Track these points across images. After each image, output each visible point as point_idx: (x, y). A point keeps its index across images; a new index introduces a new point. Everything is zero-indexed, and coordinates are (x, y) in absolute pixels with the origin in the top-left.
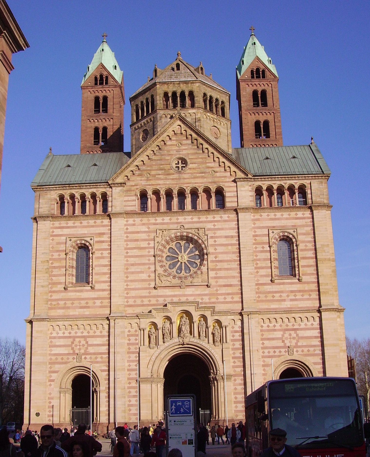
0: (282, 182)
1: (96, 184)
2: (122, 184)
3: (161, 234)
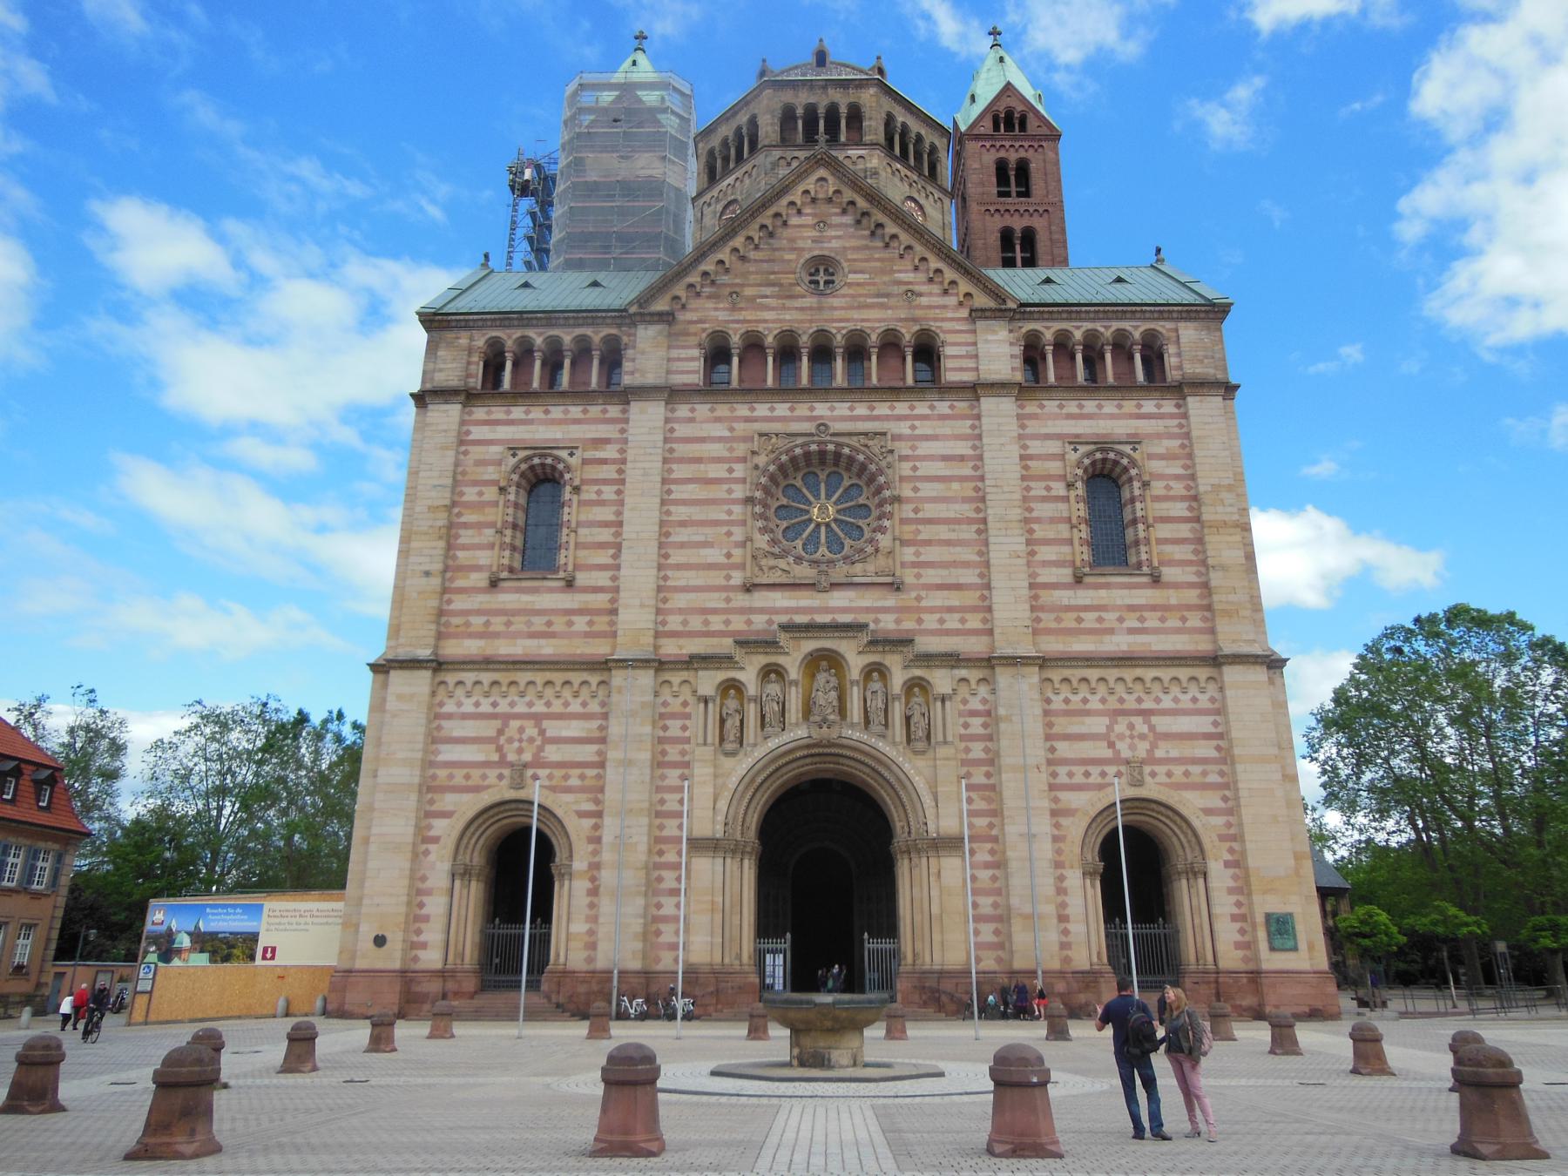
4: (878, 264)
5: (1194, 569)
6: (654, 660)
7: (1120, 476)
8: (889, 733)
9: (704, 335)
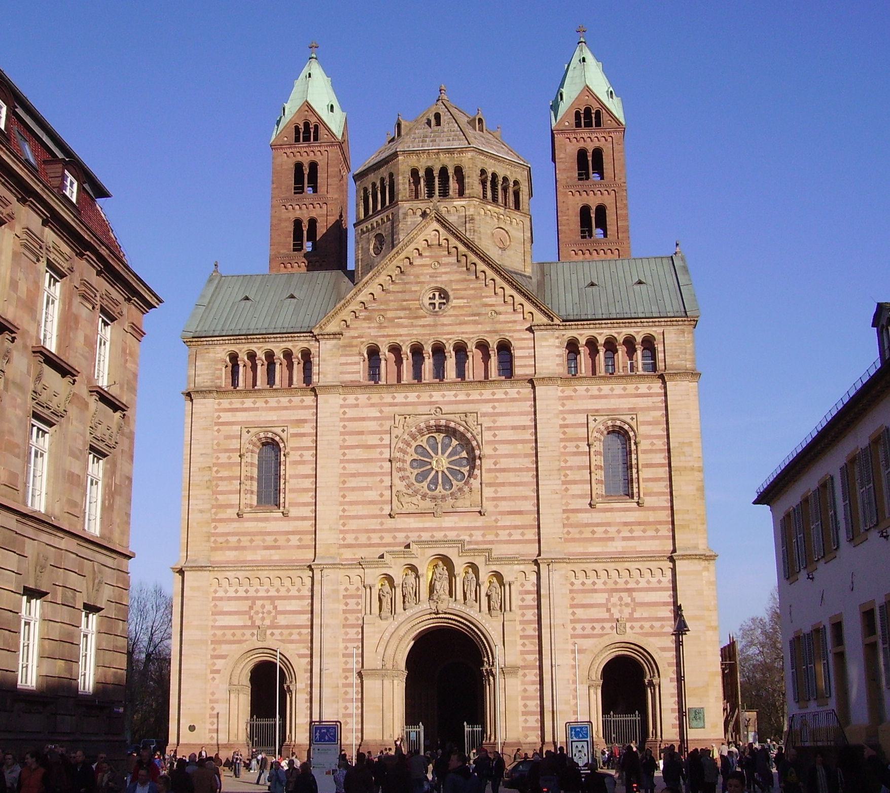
0: (613, 331)
1: (293, 335)
2: (336, 335)
3: (402, 422)
4: (472, 292)
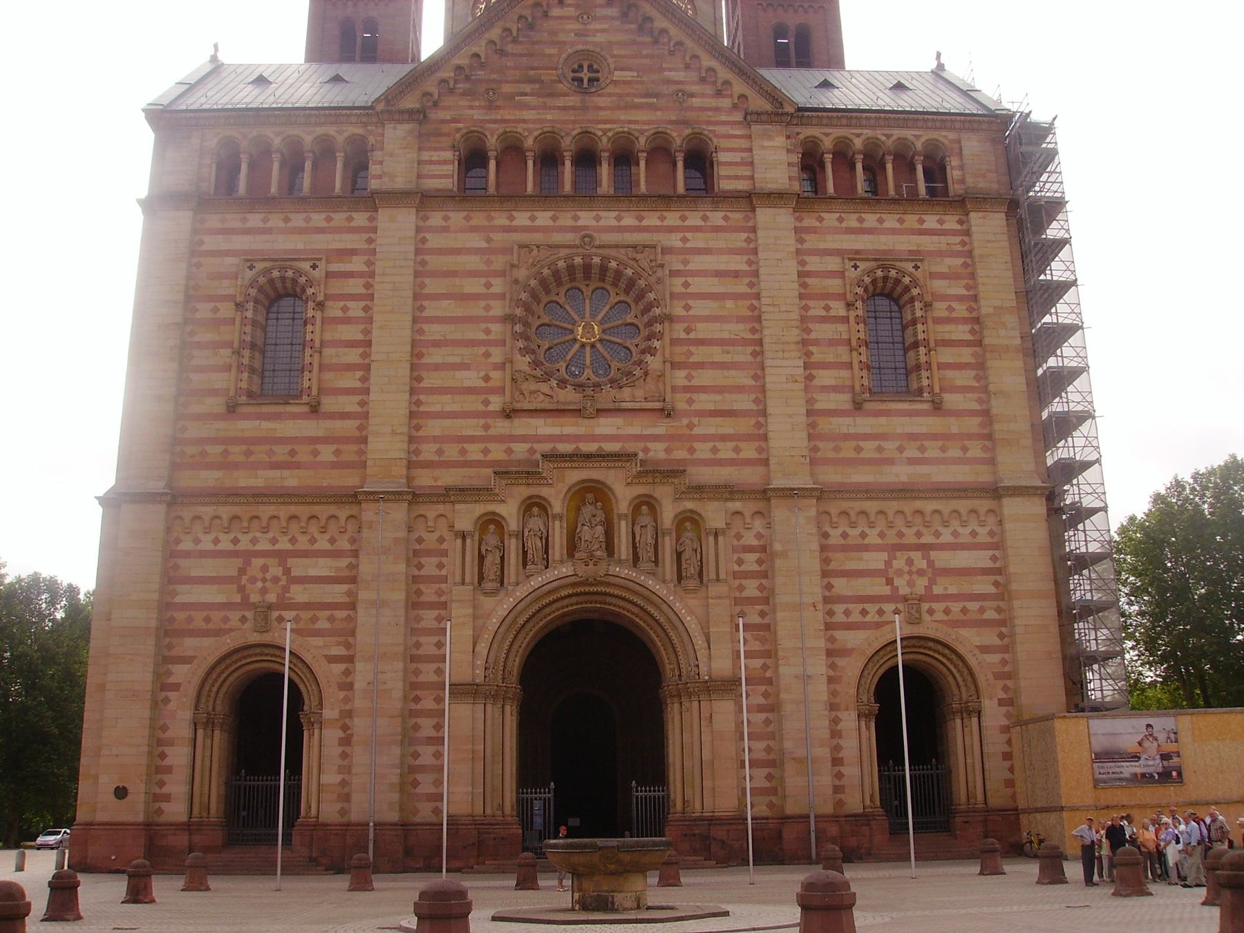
0: (878, 132)
4: (647, 61)
5: (975, 396)
6: (408, 493)
7: (901, 295)
8: (660, 569)
9: (458, 136)
